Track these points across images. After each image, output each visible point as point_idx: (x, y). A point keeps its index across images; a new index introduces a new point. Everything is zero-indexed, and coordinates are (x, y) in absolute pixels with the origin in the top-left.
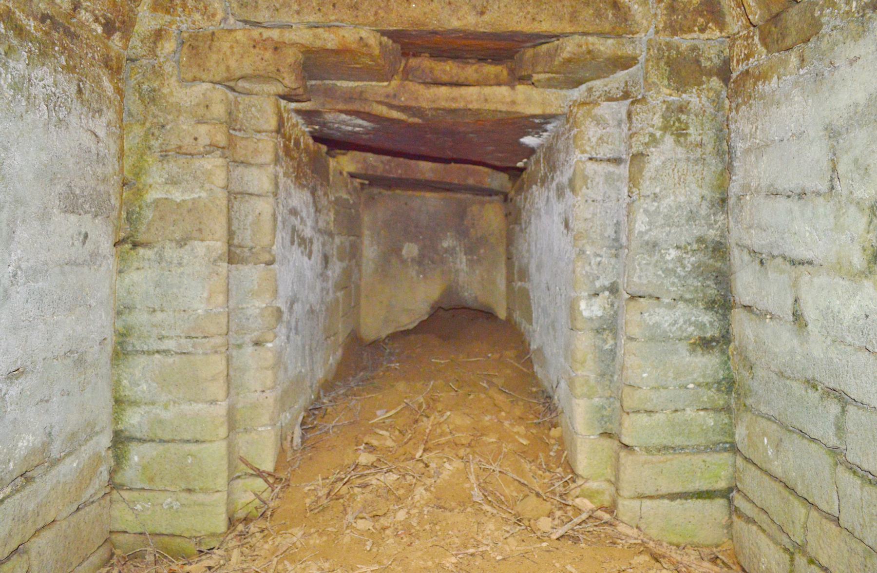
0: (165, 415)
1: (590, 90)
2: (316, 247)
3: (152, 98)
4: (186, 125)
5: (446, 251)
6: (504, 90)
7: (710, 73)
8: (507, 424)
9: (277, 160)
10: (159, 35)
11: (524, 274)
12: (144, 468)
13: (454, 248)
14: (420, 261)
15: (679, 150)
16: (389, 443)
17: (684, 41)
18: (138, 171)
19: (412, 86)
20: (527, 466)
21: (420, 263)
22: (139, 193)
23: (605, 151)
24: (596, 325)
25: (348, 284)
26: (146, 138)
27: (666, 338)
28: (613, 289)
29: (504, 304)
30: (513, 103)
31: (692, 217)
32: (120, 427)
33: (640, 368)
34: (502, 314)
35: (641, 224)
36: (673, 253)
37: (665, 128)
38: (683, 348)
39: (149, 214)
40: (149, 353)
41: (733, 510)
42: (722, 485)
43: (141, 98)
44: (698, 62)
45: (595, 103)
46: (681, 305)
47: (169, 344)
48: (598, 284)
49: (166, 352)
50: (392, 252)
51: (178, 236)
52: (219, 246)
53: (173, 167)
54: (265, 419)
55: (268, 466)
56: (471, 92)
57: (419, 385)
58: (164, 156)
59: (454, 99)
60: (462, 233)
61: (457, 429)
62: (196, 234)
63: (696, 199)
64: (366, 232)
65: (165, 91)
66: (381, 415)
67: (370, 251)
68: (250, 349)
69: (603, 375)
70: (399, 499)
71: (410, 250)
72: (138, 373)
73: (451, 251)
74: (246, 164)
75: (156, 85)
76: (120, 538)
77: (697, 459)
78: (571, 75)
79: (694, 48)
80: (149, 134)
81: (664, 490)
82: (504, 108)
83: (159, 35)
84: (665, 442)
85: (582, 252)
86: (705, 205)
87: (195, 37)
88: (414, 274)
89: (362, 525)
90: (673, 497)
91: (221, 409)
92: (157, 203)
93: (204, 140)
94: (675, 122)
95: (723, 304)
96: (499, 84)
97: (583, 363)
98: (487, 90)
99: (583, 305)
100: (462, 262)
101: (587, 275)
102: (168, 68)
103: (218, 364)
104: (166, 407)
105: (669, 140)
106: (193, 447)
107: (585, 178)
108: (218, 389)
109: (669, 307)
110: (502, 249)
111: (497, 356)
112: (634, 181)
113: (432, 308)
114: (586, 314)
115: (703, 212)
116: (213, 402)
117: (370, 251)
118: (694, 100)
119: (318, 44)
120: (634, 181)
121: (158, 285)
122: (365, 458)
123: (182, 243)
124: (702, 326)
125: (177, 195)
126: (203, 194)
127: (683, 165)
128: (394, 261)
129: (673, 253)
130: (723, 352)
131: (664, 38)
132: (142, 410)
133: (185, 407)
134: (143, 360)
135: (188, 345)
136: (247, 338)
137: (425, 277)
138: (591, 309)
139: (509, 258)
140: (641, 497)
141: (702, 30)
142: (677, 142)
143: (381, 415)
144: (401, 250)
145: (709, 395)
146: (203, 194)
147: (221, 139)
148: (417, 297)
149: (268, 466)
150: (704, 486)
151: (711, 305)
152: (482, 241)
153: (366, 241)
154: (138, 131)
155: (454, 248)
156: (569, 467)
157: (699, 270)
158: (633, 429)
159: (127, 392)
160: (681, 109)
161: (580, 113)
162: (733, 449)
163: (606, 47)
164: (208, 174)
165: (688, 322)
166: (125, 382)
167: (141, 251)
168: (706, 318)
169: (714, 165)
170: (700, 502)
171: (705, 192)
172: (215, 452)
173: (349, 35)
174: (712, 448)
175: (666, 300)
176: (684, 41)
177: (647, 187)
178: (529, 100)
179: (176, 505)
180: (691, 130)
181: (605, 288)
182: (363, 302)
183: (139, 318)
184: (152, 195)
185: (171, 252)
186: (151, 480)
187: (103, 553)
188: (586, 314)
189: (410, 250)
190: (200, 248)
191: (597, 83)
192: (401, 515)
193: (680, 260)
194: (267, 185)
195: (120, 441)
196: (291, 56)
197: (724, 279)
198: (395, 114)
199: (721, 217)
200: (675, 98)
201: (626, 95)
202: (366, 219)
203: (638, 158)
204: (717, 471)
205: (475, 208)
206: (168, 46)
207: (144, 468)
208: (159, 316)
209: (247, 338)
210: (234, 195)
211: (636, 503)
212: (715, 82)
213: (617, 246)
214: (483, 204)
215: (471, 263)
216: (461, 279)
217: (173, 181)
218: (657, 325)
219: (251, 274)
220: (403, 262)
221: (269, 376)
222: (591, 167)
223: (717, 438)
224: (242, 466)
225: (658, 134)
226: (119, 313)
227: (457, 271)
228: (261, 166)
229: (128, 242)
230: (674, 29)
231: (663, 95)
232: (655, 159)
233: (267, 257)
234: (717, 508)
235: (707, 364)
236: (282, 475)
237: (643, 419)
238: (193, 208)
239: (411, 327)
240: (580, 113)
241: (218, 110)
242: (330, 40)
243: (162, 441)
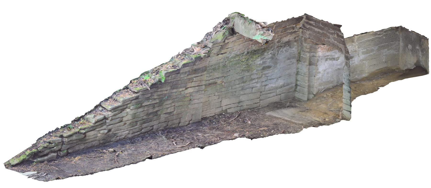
3: (302, 44)
10: (302, 37)
21: (412, 51)
52: (307, 63)
53: (303, 53)
55: (315, 94)
83: (302, 37)
91: (307, 84)
103: (307, 78)
108: (307, 82)
123: (304, 62)
128: (407, 48)
172: (306, 90)
183: (299, 70)
185: (303, 63)
195: (296, 85)
217: (303, 54)
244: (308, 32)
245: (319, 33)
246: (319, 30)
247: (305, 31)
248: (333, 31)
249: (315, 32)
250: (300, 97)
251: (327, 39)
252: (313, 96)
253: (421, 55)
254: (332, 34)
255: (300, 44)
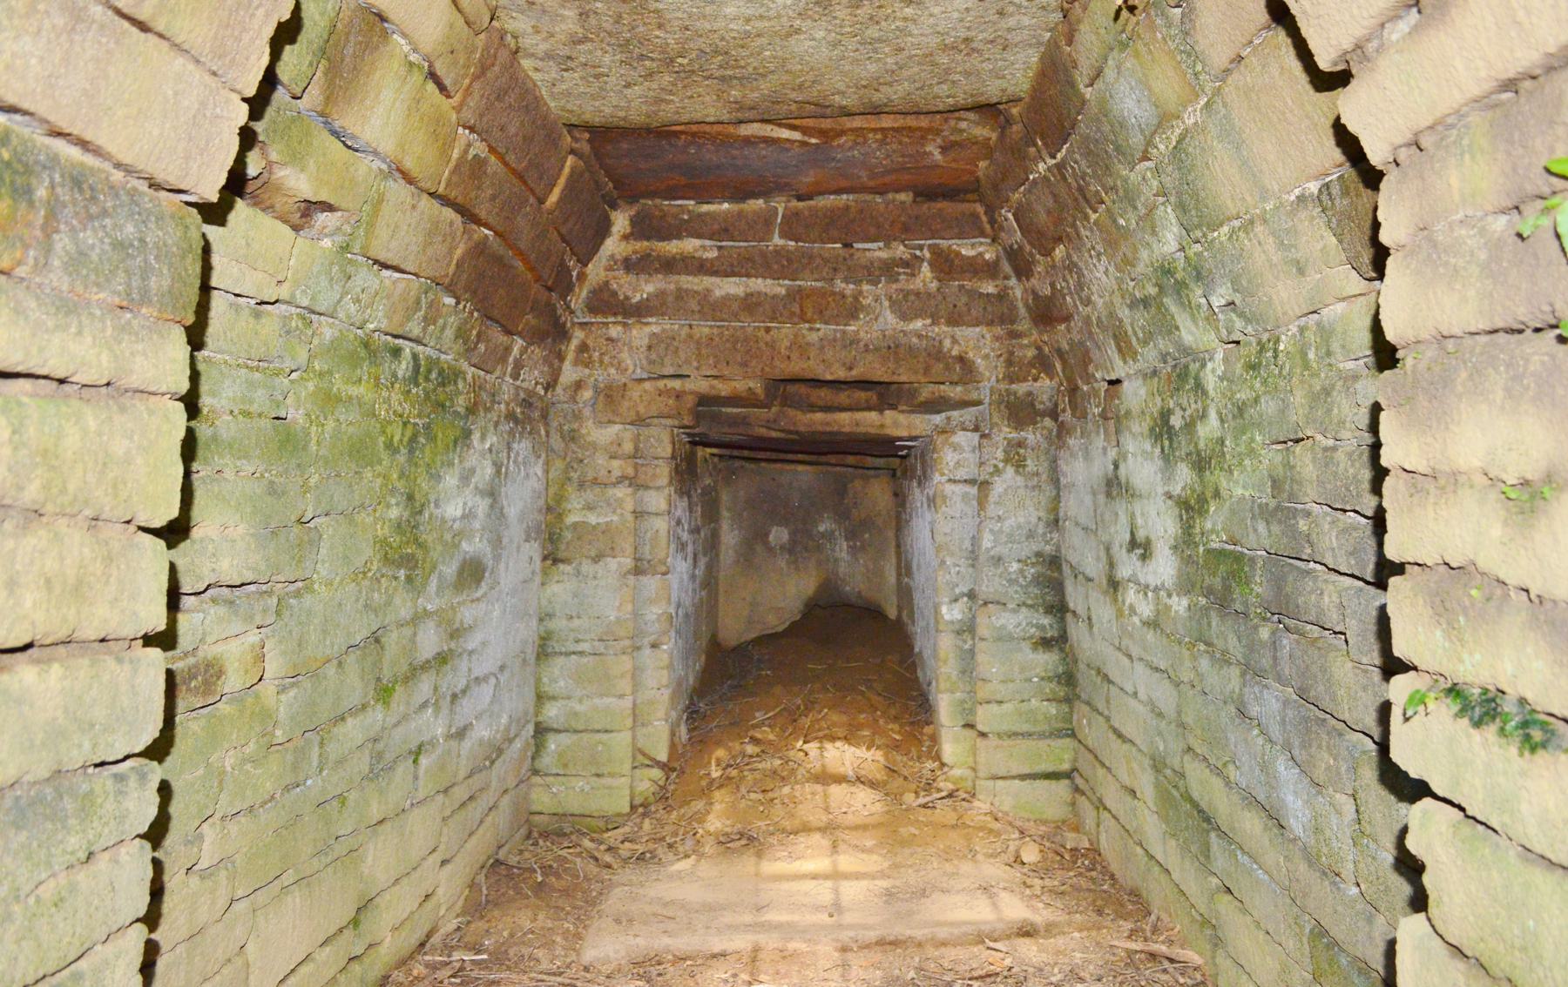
0: (578, 708)
1: (948, 418)
2: (690, 549)
3: (572, 437)
4: (601, 460)
5: (823, 535)
6: (873, 415)
7: (1043, 414)
8: (881, 722)
9: (670, 483)
10: (578, 385)
11: (909, 573)
12: (560, 755)
13: (833, 532)
14: (791, 549)
15: (1019, 478)
16: (771, 737)
17: (1021, 388)
18: (560, 498)
19: (791, 412)
20: (899, 758)
21: (791, 552)
22: (560, 517)
23: (962, 474)
24: (957, 627)
25: (709, 582)
26: (566, 471)
27: (1011, 638)
28: (971, 595)
29: (894, 600)
30: (882, 426)
31: (1031, 535)
32: (540, 719)
33: (990, 664)
34: (892, 613)
35: (987, 541)
36: (1015, 566)
37: (1006, 461)
38: (1026, 647)
39: (568, 535)
40: (568, 654)
41: (1077, 789)
42: (1066, 767)
43: (562, 437)
44: (1033, 405)
45: (953, 432)
46: (1024, 609)
47: (585, 646)
48: (957, 591)
49: (581, 653)
50: (756, 538)
51: (593, 554)
52: (628, 562)
53: (589, 495)
54: (661, 714)
55: (663, 756)
56: (844, 417)
57: (795, 689)
58: (581, 485)
59: (828, 424)
60: (842, 515)
61: (834, 724)
62: (608, 551)
63: (1034, 520)
64: (725, 514)
65: (584, 431)
66: (759, 716)
67: (730, 537)
68: (647, 651)
69: (964, 672)
70: (783, 779)
71: (779, 535)
72: (557, 672)
73: (829, 536)
74: (647, 488)
75: (575, 426)
76: (536, 818)
77: (1043, 744)
78: (936, 405)
79: (1030, 394)
80: (569, 467)
81: (1014, 772)
82: (873, 431)
84: (1014, 729)
85: (943, 562)
86: (1041, 525)
87: (609, 387)
88: (783, 565)
89: (753, 796)
90: (1023, 777)
91: (627, 703)
92: (575, 525)
93: (617, 473)
94: (1015, 456)
95: (1059, 609)
96: (869, 409)
97: (945, 662)
98: (859, 415)
99: (944, 609)
100: (842, 550)
101: (948, 583)
102: (587, 412)
104: (580, 701)
105: (1010, 470)
106: (605, 737)
107: (944, 498)
108: (625, 685)
109: (1014, 611)
110: (891, 534)
111: (878, 661)
112: (982, 502)
113: (806, 605)
114: (947, 617)
115: (1040, 531)
116: (621, 696)
117: (730, 537)
118: (1031, 437)
119: (714, 392)
120: (982, 502)
121: (575, 595)
122: (751, 749)
123: (596, 559)
124: (1042, 628)
125: (593, 519)
126: (615, 518)
127: (1021, 491)
128: (759, 548)
129: (1015, 566)
130: (1062, 650)
131: (1003, 386)
132: (559, 704)
133: (597, 701)
134: (560, 660)
135: (601, 647)
136: (646, 641)
137: (797, 569)
138: (952, 613)
139: (898, 546)
140: (996, 778)
141: (1035, 380)
142: (1017, 472)
143: (759, 716)
144: (767, 535)
145: (1049, 687)
146: (615, 518)
147: (630, 471)
148: (785, 592)
149: (663, 756)
150: (1050, 768)
151: (1049, 610)
152: (867, 524)
153: (725, 526)
154: (559, 464)
155: (833, 532)
156: (938, 757)
157: (1037, 580)
158: (985, 717)
159: (547, 689)
160: (1020, 444)
161: (939, 440)
162: (1073, 735)
163: (956, 392)
164: (620, 501)
165: (1030, 624)
166: (545, 680)
167: (561, 566)
168: (1046, 621)
169: (1049, 491)
170: (1046, 782)
171: (1042, 514)
172: (621, 742)
173: (740, 386)
174: (1057, 734)
175: (1010, 606)
176: (1021, 388)
177: (992, 510)
178: (896, 424)
179: (587, 788)
180: (1029, 462)
181: (964, 595)
182: (721, 599)
183: (557, 624)
184: (571, 519)
185: (587, 567)
186: (565, 766)
187: (523, 831)
188: (947, 617)
189: (779, 535)
190: (612, 564)
191: (955, 414)
192: (786, 790)
193: (1021, 571)
194: (663, 506)
195: (541, 731)
196: (690, 401)
197: (1058, 587)
198: (774, 434)
199: (1056, 535)
200: (1014, 435)
201: (976, 429)
202: (725, 497)
203: (984, 486)
204: (1060, 754)
205: (858, 484)
206: (587, 394)
207: (560, 755)
208: (576, 622)
209: (646, 641)
210: (639, 514)
211: (990, 783)
212: (1048, 422)
213: (973, 556)
214: (866, 479)
215: (853, 550)
216: (841, 570)
217: (589, 507)
218: (1003, 627)
219: (651, 583)
220: (770, 550)
221: (658, 678)
222: (949, 488)
223: (1061, 725)
224: (640, 757)
225: (1001, 465)
226: (541, 620)
227: (836, 560)
228: (658, 488)
229: (552, 558)
230: (1011, 378)
231: (1005, 433)
232: (999, 486)
233: (664, 569)
234: (1061, 788)
235: (1047, 660)
236: (676, 765)
237: (994, 708)
238: (607, 530)
239: (780, 629)
240: (939, 440)
241: (628, 447)
242: (723, 389)
243: (576, 731)
244: (640, 334)
245: (750, 304)
246: (759, 284)
247: (615, 331)
248: (900, 251)
249: (712, 308)
250: (574, 805)
251: (825, 329)
252: (657, 773)
253: (844, 555)
254: (888, 269)
255: (556, 442)
